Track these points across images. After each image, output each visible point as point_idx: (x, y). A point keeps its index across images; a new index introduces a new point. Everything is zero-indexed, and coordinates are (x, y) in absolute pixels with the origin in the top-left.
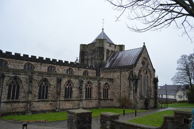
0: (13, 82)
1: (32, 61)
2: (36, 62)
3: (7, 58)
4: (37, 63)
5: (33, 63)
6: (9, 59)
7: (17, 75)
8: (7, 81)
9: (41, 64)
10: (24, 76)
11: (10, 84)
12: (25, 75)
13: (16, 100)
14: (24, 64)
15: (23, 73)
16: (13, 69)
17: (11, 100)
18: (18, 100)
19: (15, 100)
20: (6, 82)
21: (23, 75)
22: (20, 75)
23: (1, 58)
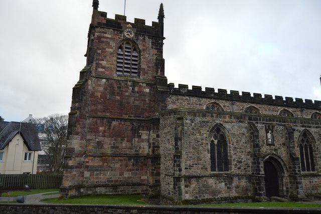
0: (303, 141)
1: (289, 107)
2: (294, 107)
3: (257, 103)
4: (295, 109)
5: (290, 110)
6: (260, 106)
7: (307, 129)
8: (296, 138)
9: (302, 111)
10: (316, 130)
11: (301, 145)
12: (317, 127)
13: (307, 172)
14: (279, 112)
15: (313, 124)
16: (300, 119)
17: (306, 172)
18: (316, 172)
19: (312, 172)
20: (297, 141)
21: (314, 127)
22: (310, 127)
23: (251, 105)
